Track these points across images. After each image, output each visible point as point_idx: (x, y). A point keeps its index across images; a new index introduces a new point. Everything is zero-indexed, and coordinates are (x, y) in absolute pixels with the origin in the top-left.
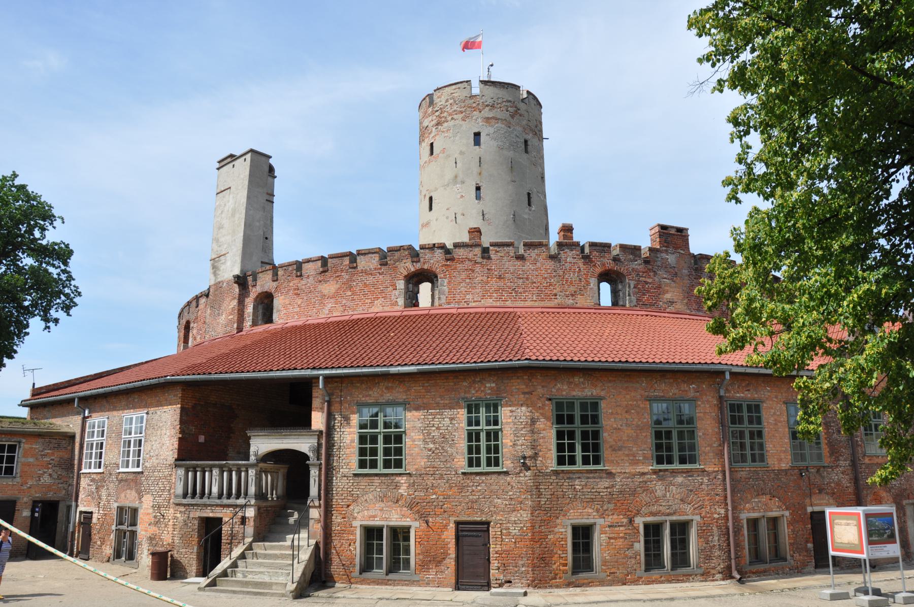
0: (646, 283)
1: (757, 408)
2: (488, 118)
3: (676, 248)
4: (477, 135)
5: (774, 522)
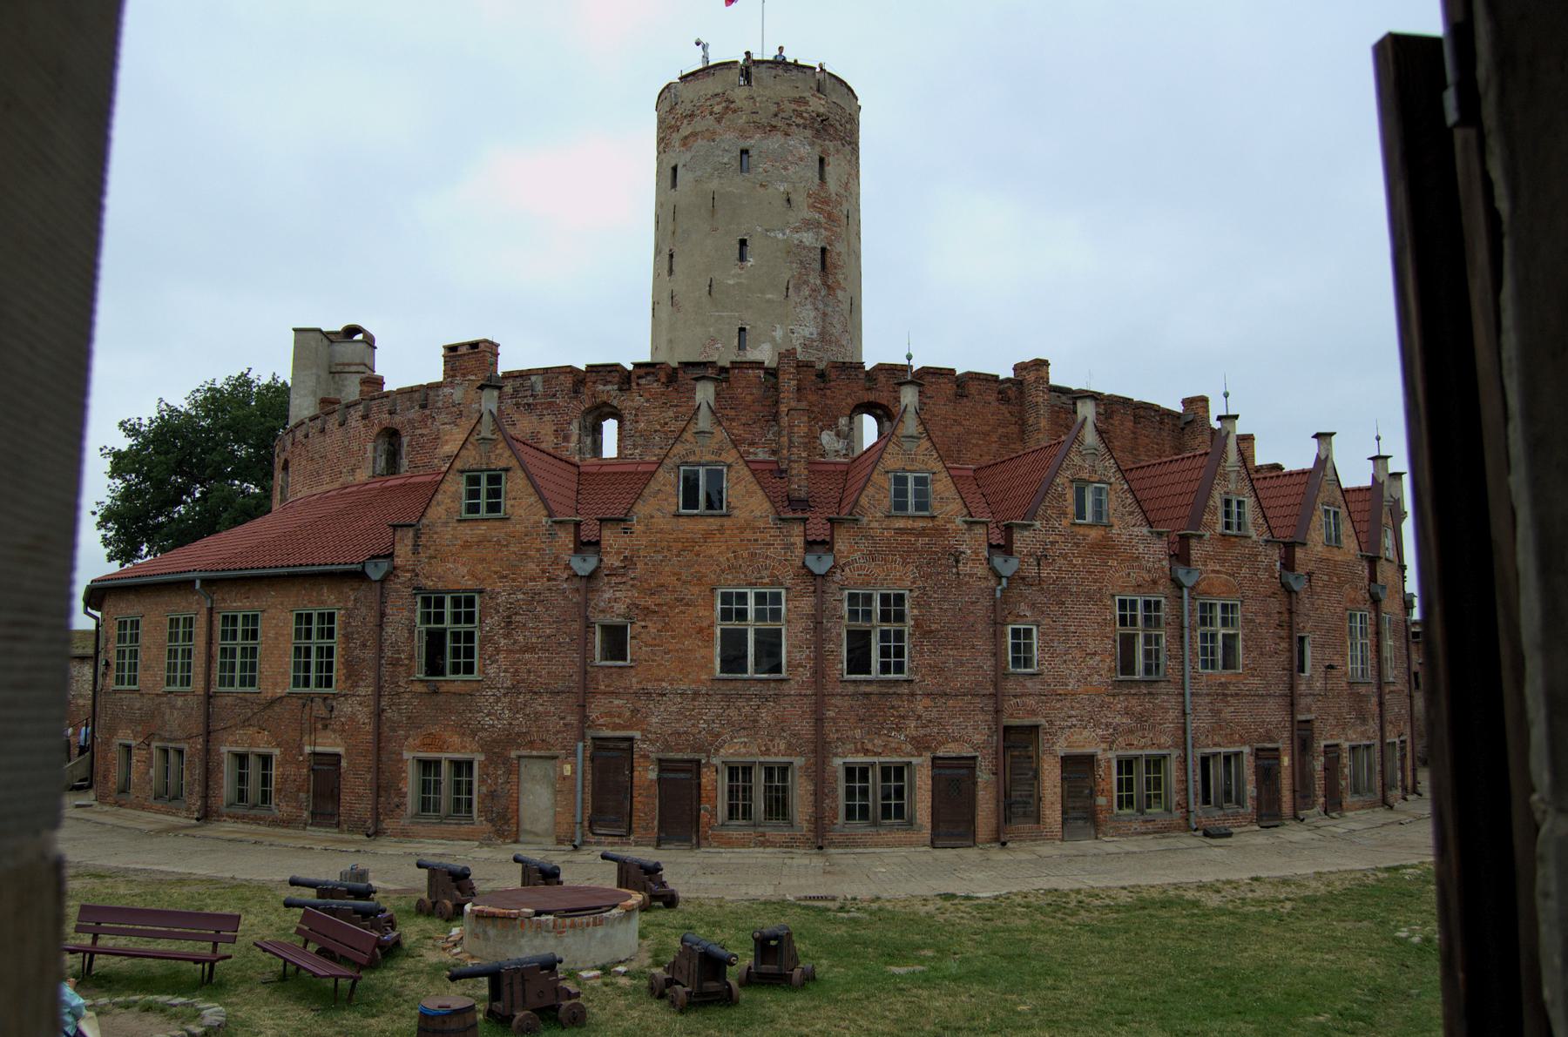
0: (422, 435)
1: (255, 617)
3: (464, 375)
4: (675, 169)
5: (266, 760)
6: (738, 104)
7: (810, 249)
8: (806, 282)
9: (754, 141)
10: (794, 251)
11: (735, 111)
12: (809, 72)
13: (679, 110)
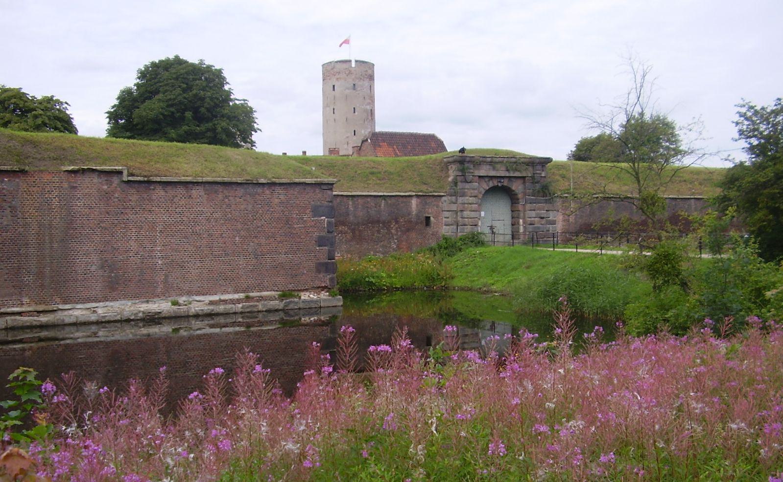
4: (334, 86)
9: (356, 82)
10: (365, 111)
13: (335, 70)
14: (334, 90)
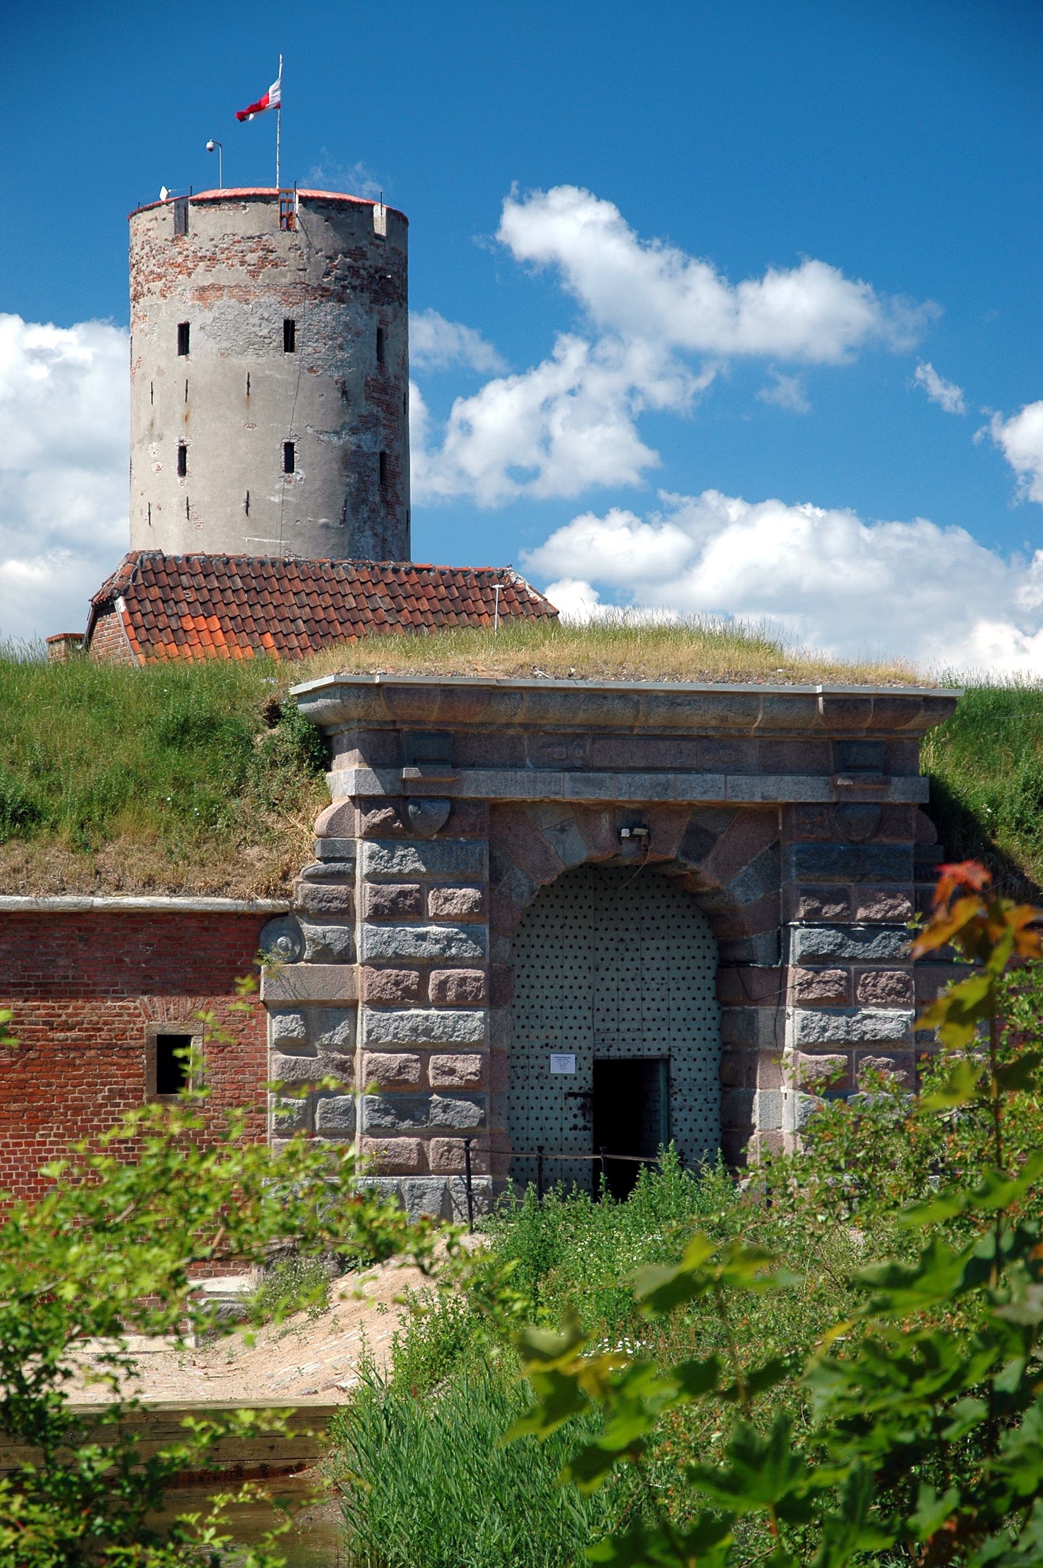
2: (203, 289)
4: (184, 330)
6: (280, 253)
7: (368, 456)
8: (364, 501)
11: (276, 266)
12: (366, 210)
13: (189, 244)
14: (184, 347)
